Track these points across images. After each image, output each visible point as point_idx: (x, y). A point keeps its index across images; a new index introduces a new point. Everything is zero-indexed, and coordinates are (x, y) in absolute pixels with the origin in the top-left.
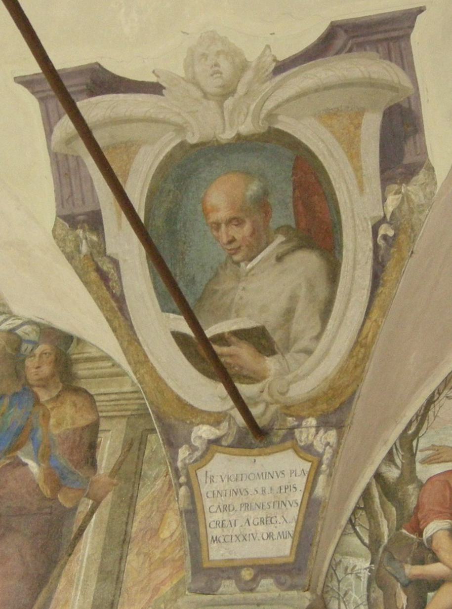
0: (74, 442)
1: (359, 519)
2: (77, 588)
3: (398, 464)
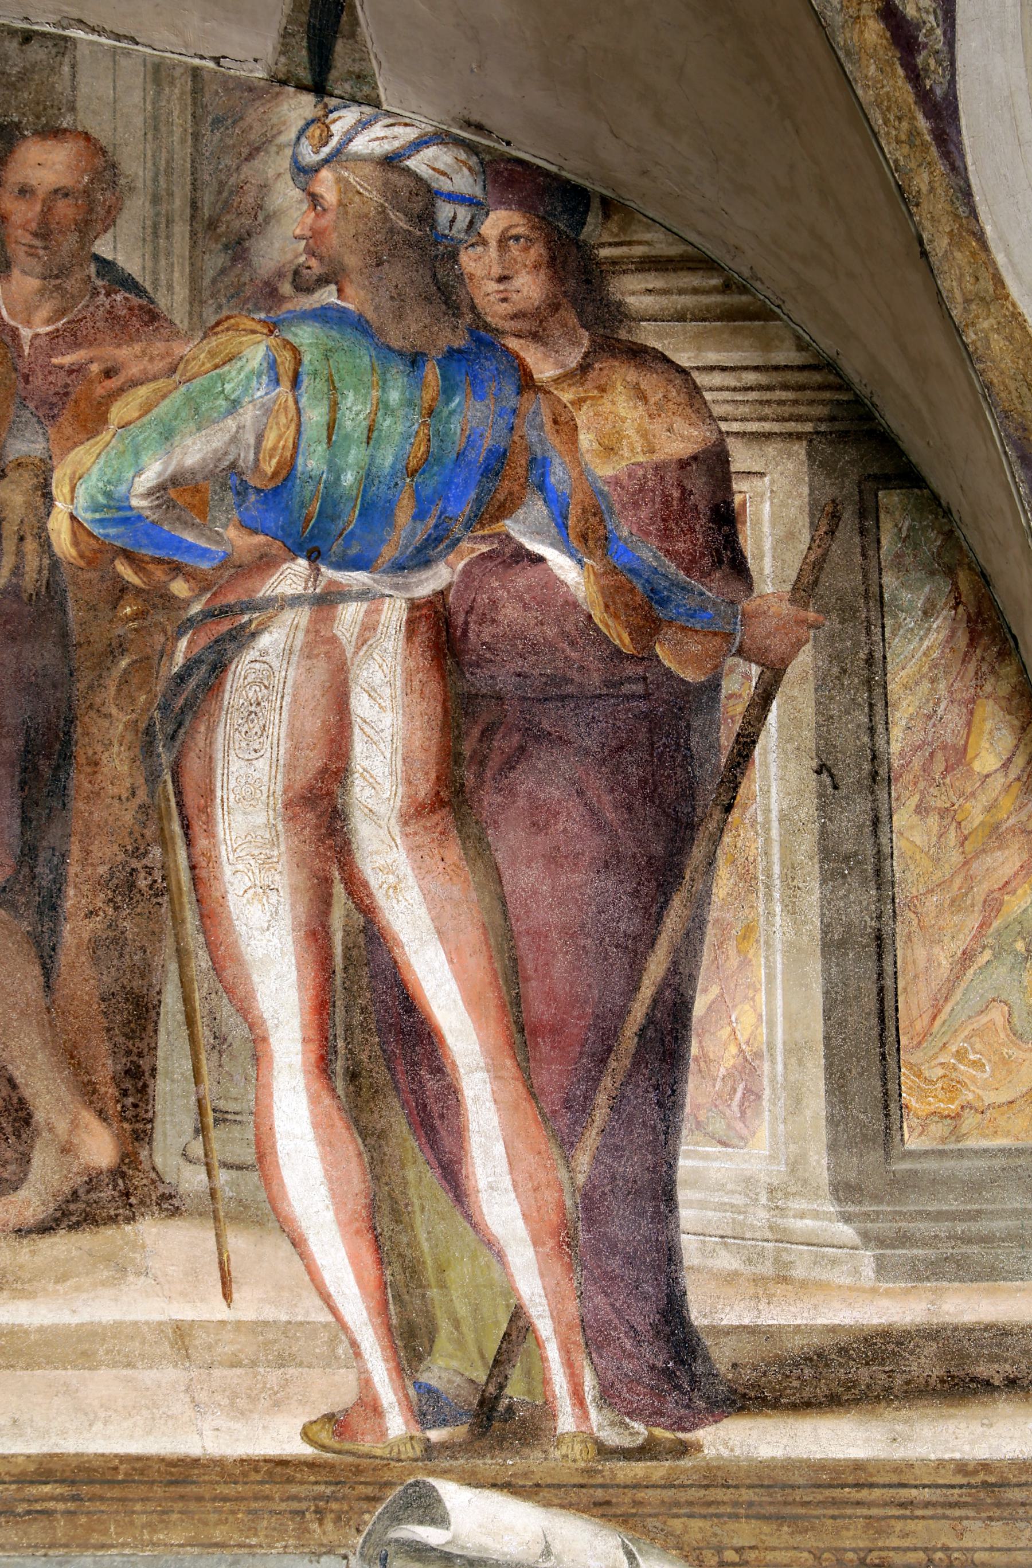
0: (666, 502)
2: (769, 897)
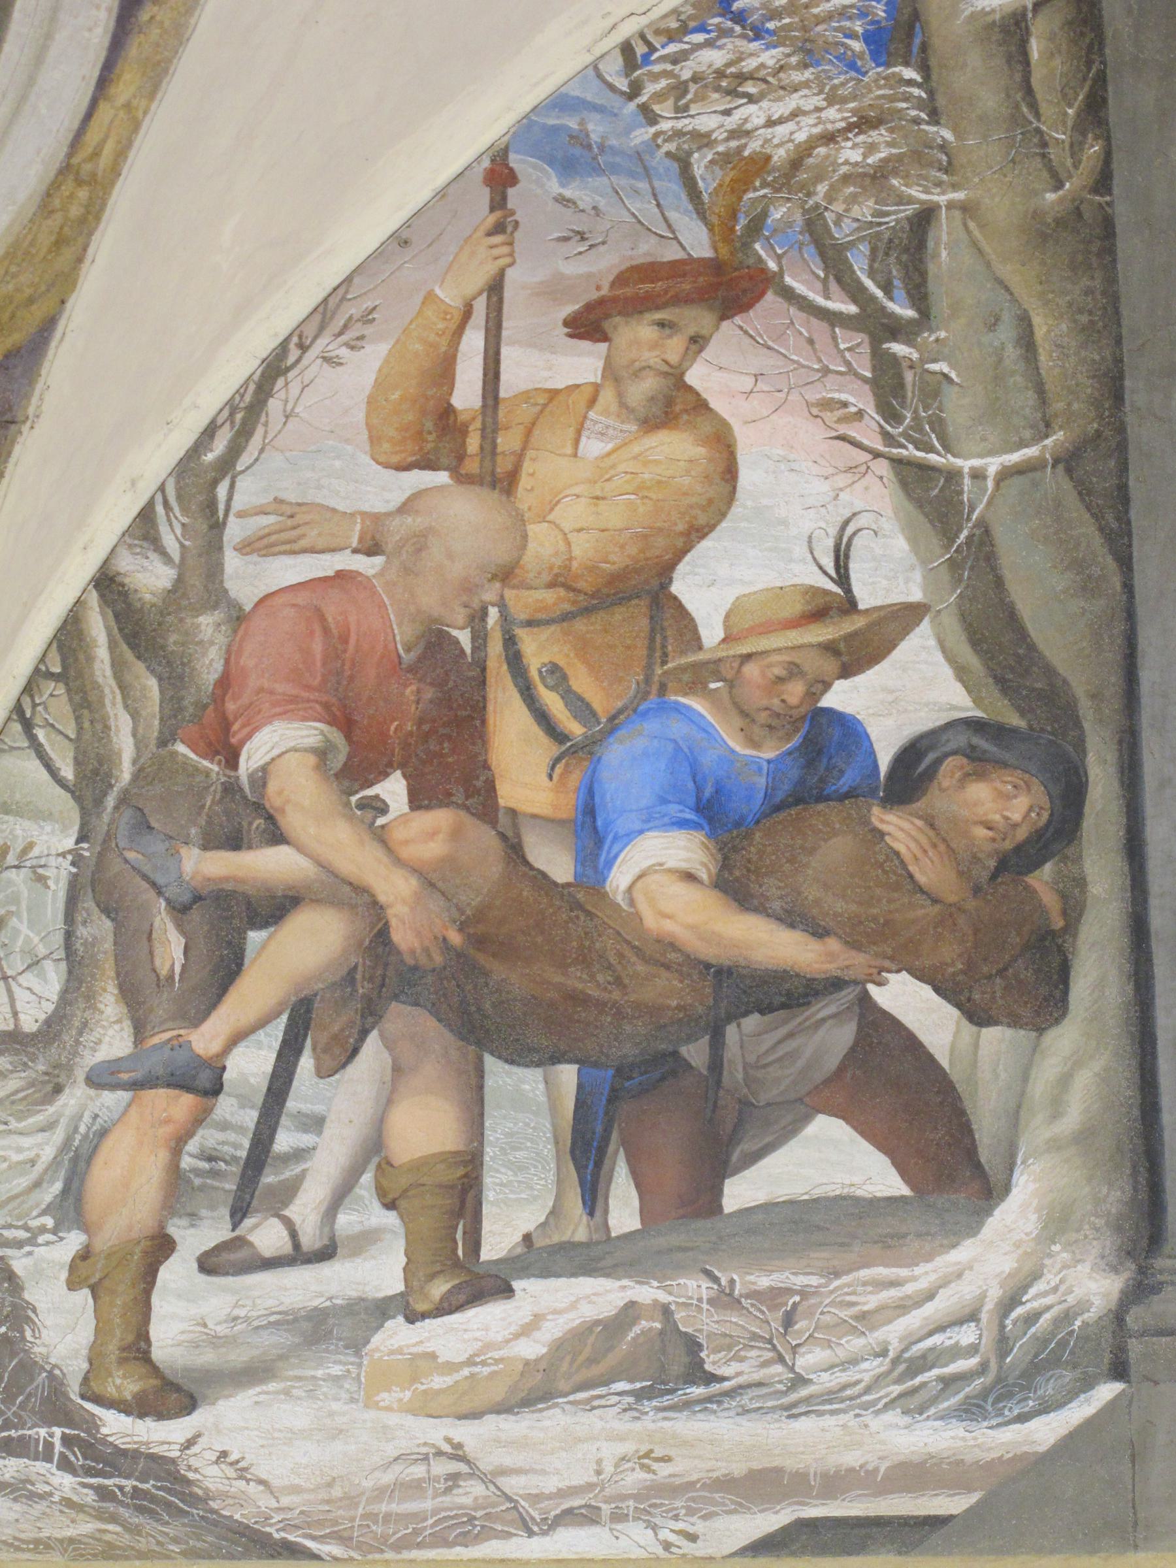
1: (46, 709)
3: (169, 550)
